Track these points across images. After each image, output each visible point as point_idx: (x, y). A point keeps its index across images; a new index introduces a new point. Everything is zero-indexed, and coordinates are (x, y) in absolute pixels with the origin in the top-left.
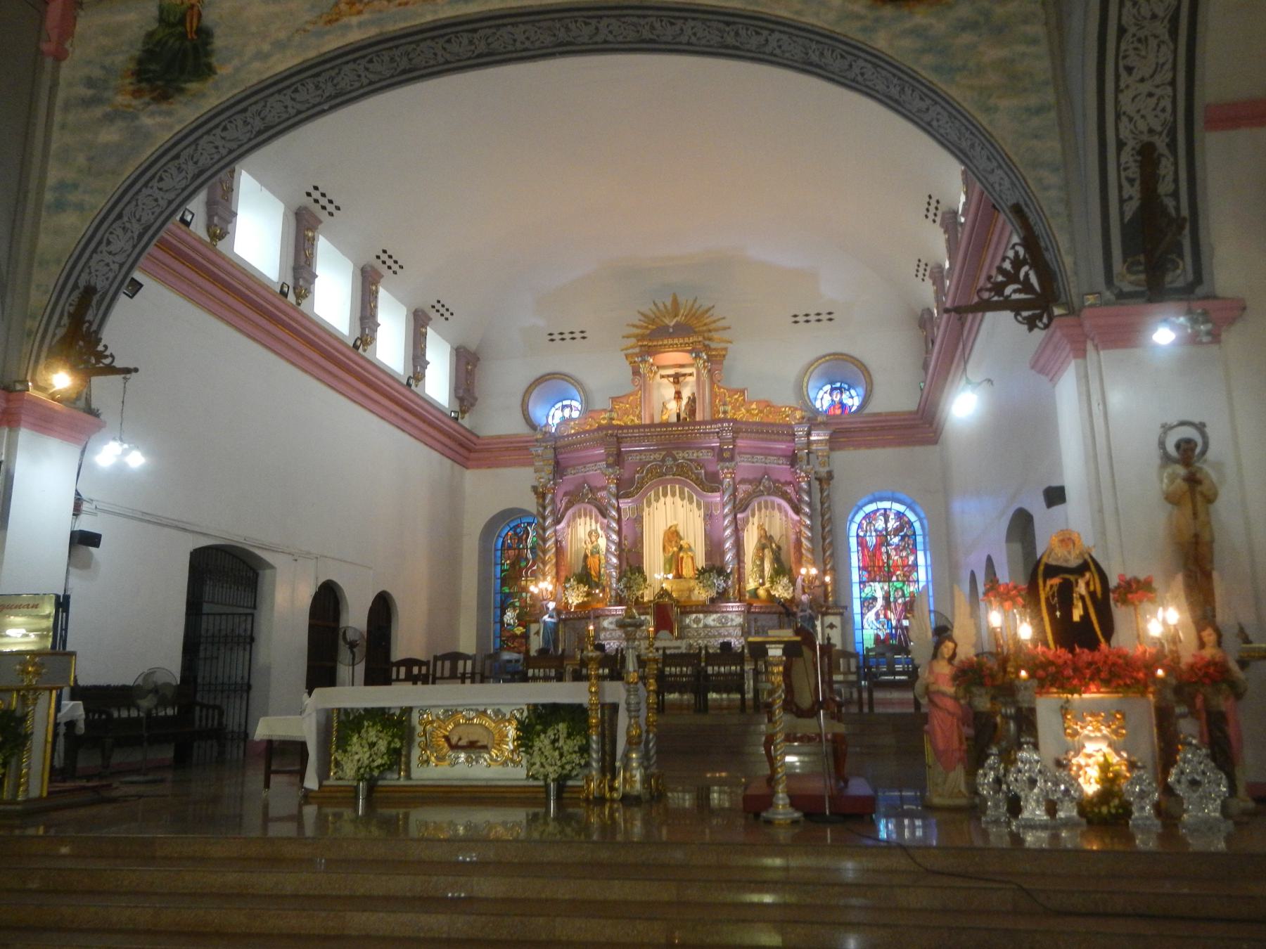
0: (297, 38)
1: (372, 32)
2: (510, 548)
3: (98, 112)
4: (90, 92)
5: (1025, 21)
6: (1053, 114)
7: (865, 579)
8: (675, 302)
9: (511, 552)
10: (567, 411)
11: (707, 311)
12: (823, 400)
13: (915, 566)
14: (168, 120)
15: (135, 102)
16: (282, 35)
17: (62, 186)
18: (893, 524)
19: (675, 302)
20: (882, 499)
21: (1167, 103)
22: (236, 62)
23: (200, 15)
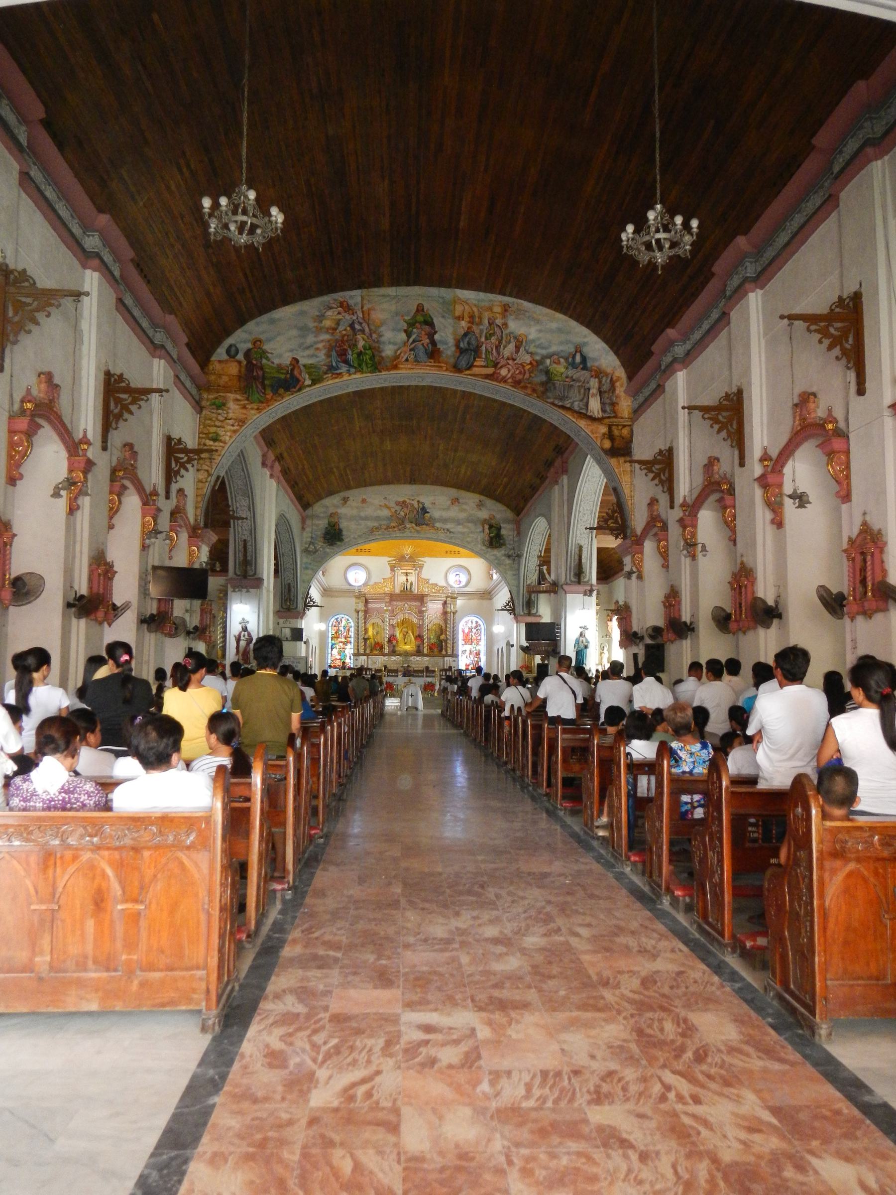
18: (474, 625)
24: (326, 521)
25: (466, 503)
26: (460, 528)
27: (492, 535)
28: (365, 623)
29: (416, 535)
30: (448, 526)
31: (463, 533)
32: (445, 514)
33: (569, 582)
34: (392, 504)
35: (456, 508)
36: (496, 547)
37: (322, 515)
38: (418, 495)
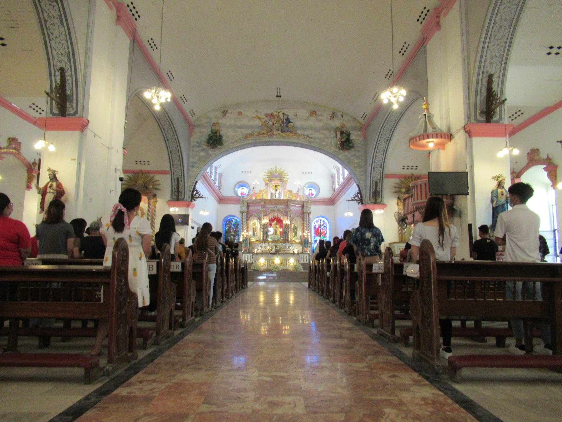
0: (239, 140)
1: (254, 141)
2: (228, 224)
3: (200, 149)
4: (198, 145)
5: (361, 156)
6: (364, 172)
7: (315, 235)
8: (276, 167)
9: (228, 225)
10: (243, 189)
11: (283, 171)
12: (307, 192)
13: (326, 233)
14: (214, 153)
15: (208, 148)
16: (236, 139)
17: (193, 162)
18: (322, 223)
19: (276, 167)
20: (320, 217)
21: (379, 176)
22: (228, 143)
23: (219, 133)
24: (210, 129)
25: (321, 115)
26: (317, 135)
27: (343, 140)
28: (247, 220)
29: (282, 140)
30: (308, 133)
31: (320, 139)
32: (305, 124)
33: (475, 122)
34: (263, 116)
35: (313, 118)
36: (347, 149)
37: (206, 125)
38: (283, 109)
